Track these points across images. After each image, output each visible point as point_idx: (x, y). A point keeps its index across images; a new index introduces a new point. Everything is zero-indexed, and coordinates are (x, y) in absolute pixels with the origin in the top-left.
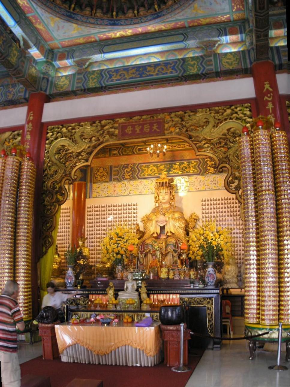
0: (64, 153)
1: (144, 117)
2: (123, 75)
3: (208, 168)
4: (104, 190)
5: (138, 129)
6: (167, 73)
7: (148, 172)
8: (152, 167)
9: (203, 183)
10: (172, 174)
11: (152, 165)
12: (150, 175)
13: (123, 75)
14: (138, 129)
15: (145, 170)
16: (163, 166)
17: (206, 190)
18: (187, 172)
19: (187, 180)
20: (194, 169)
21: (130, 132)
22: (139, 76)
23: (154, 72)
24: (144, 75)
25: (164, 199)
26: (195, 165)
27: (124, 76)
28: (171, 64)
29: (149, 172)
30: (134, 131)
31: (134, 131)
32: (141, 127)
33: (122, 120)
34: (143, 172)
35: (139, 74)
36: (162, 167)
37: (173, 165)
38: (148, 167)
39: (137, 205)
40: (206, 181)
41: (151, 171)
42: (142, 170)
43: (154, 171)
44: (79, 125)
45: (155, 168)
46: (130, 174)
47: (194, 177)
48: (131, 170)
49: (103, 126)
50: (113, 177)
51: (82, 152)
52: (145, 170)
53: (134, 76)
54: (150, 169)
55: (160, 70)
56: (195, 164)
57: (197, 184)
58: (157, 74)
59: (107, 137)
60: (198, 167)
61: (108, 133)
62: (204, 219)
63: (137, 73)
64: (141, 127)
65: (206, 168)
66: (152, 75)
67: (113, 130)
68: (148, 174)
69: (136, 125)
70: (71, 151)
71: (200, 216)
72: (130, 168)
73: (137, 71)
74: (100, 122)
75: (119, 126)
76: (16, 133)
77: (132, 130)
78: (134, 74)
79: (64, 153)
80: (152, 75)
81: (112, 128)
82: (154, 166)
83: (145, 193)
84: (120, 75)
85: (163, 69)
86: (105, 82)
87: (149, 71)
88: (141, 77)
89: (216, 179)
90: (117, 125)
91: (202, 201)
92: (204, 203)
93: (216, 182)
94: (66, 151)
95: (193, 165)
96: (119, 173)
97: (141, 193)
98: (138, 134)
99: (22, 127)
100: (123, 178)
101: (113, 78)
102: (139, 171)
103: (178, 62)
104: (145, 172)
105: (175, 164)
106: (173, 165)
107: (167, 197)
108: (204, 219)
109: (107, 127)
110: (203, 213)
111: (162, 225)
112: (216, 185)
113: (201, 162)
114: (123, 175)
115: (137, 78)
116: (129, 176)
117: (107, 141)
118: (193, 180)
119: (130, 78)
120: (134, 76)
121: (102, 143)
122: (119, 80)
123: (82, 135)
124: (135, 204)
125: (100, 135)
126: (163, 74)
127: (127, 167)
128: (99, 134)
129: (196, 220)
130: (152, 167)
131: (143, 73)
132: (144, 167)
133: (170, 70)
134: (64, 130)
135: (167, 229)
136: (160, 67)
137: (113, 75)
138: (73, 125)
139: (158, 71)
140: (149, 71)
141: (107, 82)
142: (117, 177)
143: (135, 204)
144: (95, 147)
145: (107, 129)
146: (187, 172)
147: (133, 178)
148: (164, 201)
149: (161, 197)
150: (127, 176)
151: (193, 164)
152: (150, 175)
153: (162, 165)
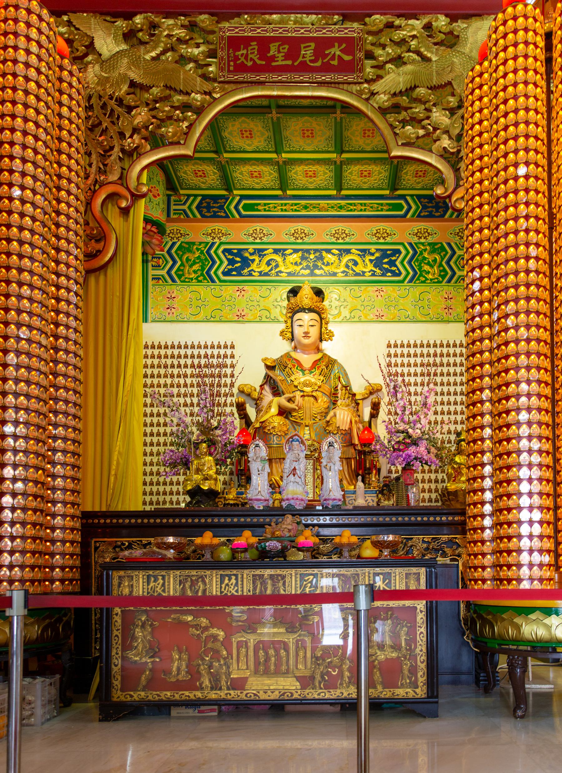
9: (394, 303)
10: (321, 275)
11: (271, 251)
12: (266, 274)
15: (253, 261)
16: (300, 254)
17: (399, 321)
18: (357, 274)
20: (375, 266)
29: (264, 268)
37: (324, 254)
38: (260, 252)
39: (233, 347)
40: (401, 301)
41: (268, 263)
52: (253, 261)
56: (377, 255)
68: (260, 272)
83: (250, 317)
89: (425, 296)
91: (389, 346)
95: (373, 258)
97: (240, 318)
104: (254, 266)
105: (328, 251)
106: (324, 254)
118: (371, 294)
124: (229, 344)
132: (251, 254)
143: (229, 344)
146: (357, 274)
151: (373, 254)
152: (266, 274)
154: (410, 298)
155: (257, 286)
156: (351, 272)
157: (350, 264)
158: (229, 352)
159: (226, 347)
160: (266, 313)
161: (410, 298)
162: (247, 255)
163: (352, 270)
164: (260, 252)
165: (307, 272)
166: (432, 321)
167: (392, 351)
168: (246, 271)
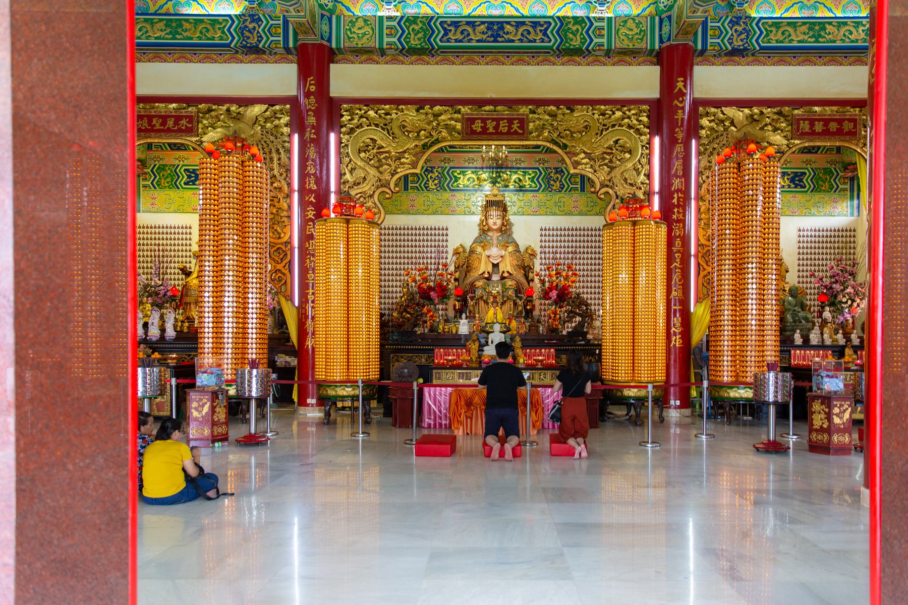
0: (375, 151)
1: (499, 108)
2: (466, 33)
4: (396, 203)
5: (491, 126)
6: (535, 41)
7: (463, 181)
8: (469, 174)
12: (467, 186)
13: (466, 33)
14: (491, 126)
19: (521, 198)
21: (479, 130)
22: (492, 39)
23: (516, 34)
24: (499, 39)
25: (495, 224)
26: (533, 177)
27: (469, 35)
28: (542, 26)
29: (466, 182)
30: (485, 129)
31: (485, 129)
32: (495, 123)
33: (465, 109)
34: (456, 181)
35: (492, 36)
36: (485, 176)
38: (463, 173)
39: (447, 229)
41: (468, 180)
42: (455, 177)
44: (397, 109)
45: (473, 176)
47: (530, 195)
49: (437, 116)
50: (410, 185)
51: (405, 152)
53: (484, 37)
54: (467, 177)
55: (525, 34)
57: (535, 204)
58: (521, 41)
59: (444, 133)
60: (537, 180)
61: (447, 127)
62: (543, 256)
63: (490, 33)
64: (495, 123)
65: (549, 183)
66: (513, 41)
67: (453, 122)
69: (488, 119)
70: (387, 149)
71: (538, 250)
73: (488, 28)
74: (431, 108)
75: (463, 118)
76: (277, 107)
77: (482, 127)
78: (483, 33)
79: (375, 151)
80: (513, 41)
81: (451, 119)
82: (473, 173)
84: (462, 33)
85: (529, 33)
86: (438, 40)
87: (508, 33)
88: (496, 41)
90: (459, 116)
91: (541, 230)
92: (543, 233)
93: (562, 204)
94: (379, 148)
98: (491, 134)
99: (293, 101)
100: (426, 188)
101: (450, 35)
102: (451, 179)
103: (553, 24)
104: (460, 181)
107: (499, 222)
108: (543, 256)
109: (443, 117)
110: (541, 247)
111: (495, 262)
112: (561, 209)
113: (541, 173)
115: (489, 42)
117: (444, 139)
119: (478, 41)
120: (484, 37)
121: (437, 141)
122: (461, 41)
123: (404, 127)
125: (433, 129)
126: (530, 41)
127: (432, 172)
128: (430, 127)
129: (533, 255)
130: (469, 174)
131: (499, 36)
133: (540, 36)
134: (371, 113)
135: (502, 268)
136: (524, 28)
137: (450, 31)
138: (387, 107)
139: (522, 35)
140: (508, 33)
141: (441, 41)
144: (425, 147)
145: (444, 121)
147: (440, 187)
148: (495, 227)
149: (491, 222)
150: (431, 185)
153: (485, 173)
154: (553, 201)
155: (463, 193)
158: (445, 232)
159: (443, 229)
160: (467, 209)
161: (553, 201)
164: (463, 173)
166: (565, 214)
167: (543, 233)
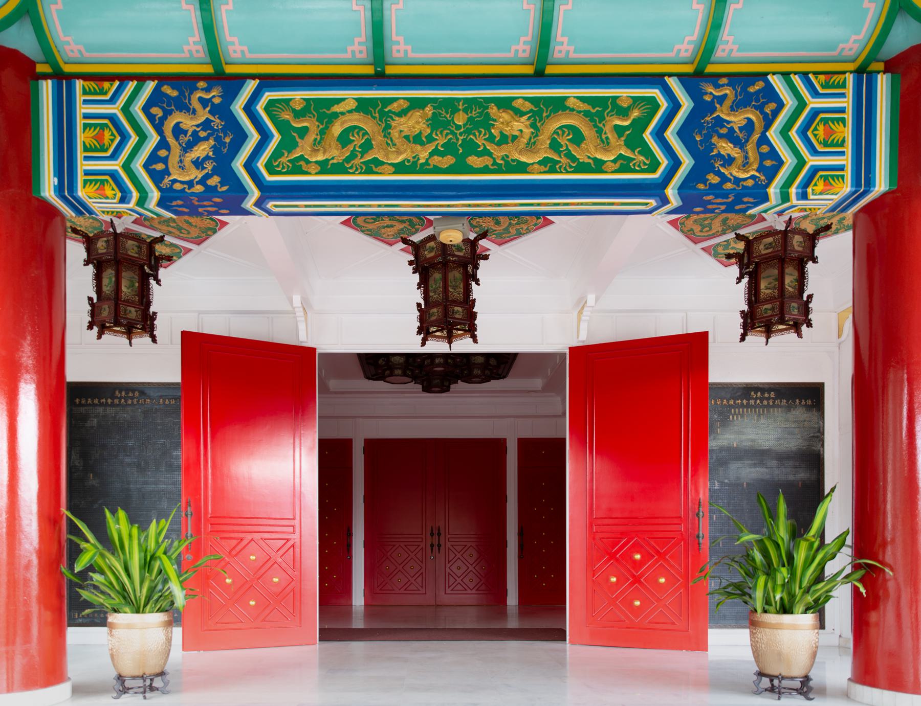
3: (726, 148)
18: (582, 168)
20: (630, 145)
43: (367, 146)
46: (202, 150)
48: (206, 125)
50: (82, 165)
52: (303, 132)
72: (203, 115)
96: (124, 137)
114: (153, 158)
116: (198, 164)
127: (183, 106)
132: (298, 115)
142: (115, 166)
151: (623, 113)
156: (564, 160)
157: (563, 141)
162: (286, 116)
163: (569, 155)
165: (449, 160)
168: (284, 160)
